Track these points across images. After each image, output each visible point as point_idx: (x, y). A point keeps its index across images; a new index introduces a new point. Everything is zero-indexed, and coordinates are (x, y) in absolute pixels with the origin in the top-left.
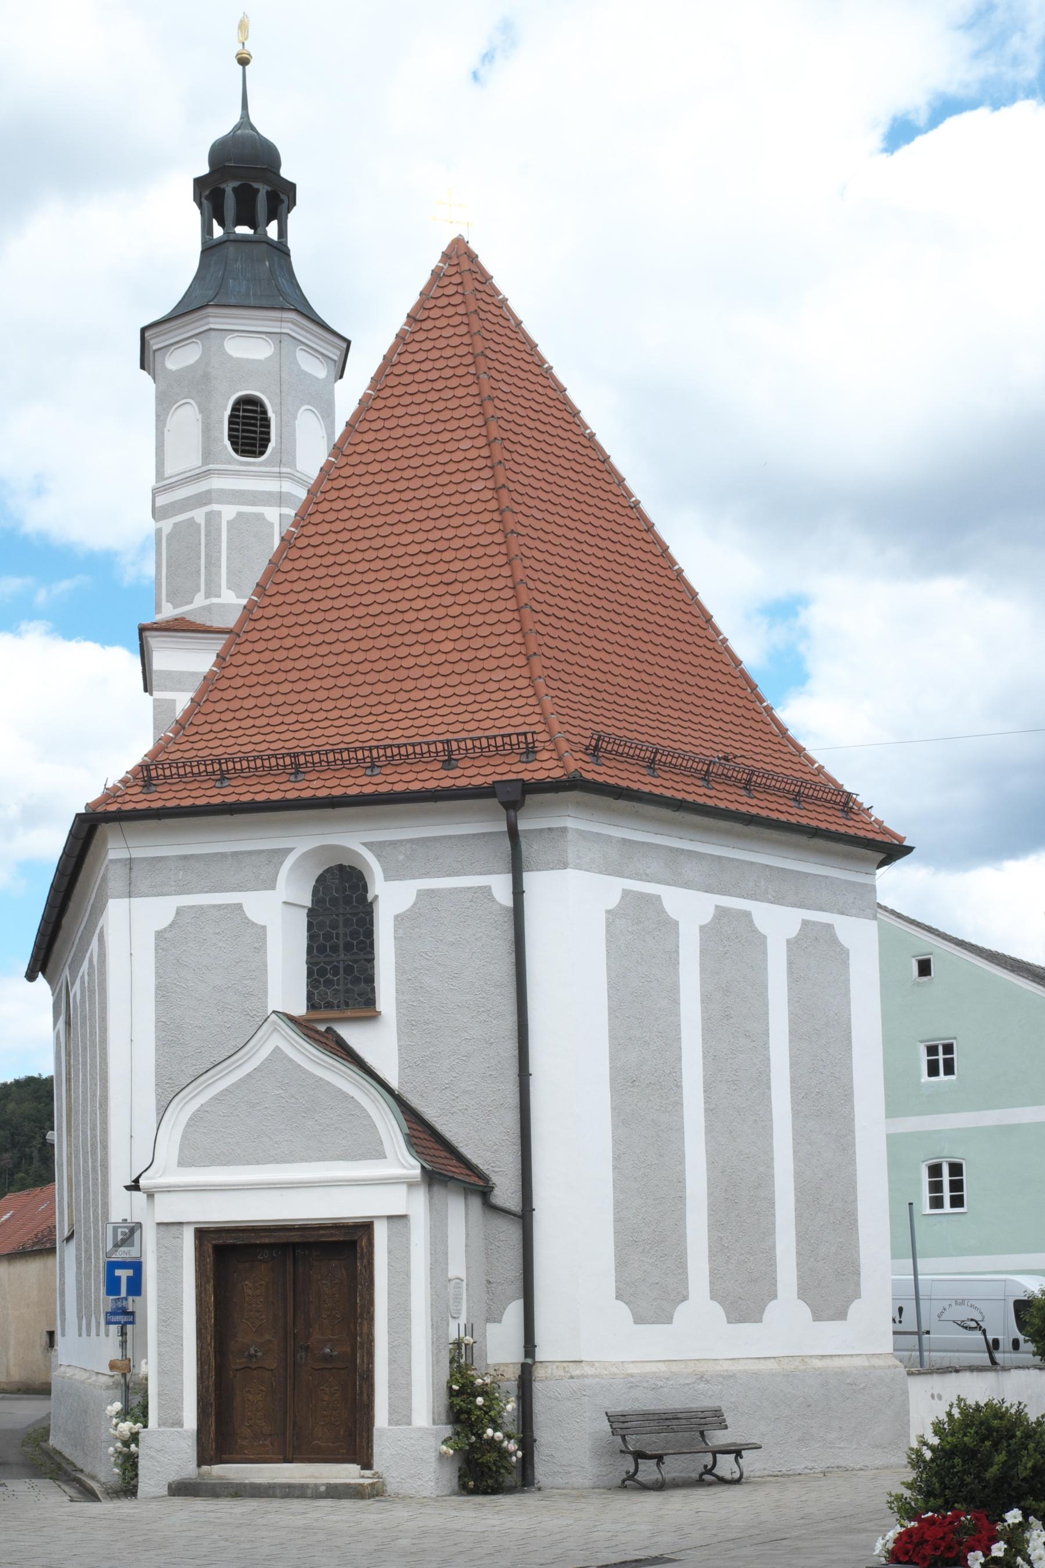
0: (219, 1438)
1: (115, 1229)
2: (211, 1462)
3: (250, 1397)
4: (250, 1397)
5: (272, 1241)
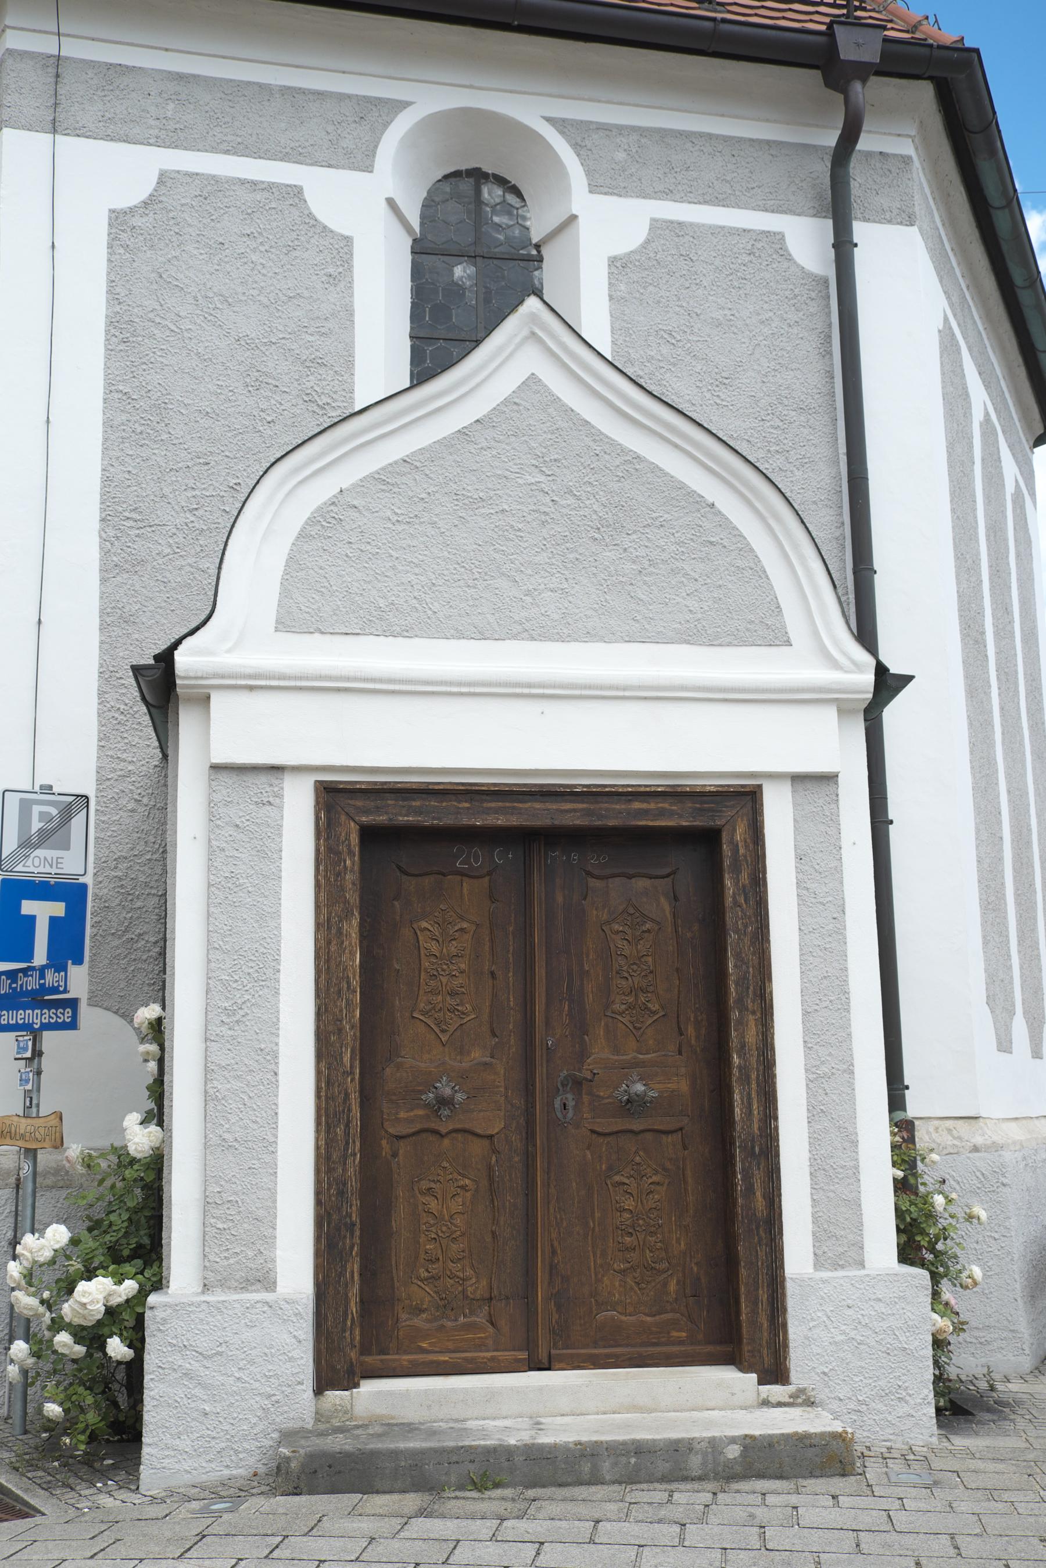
1: (25, 807)
3: (433, 1205)
4: (433, 1205)
5: (514, 821)
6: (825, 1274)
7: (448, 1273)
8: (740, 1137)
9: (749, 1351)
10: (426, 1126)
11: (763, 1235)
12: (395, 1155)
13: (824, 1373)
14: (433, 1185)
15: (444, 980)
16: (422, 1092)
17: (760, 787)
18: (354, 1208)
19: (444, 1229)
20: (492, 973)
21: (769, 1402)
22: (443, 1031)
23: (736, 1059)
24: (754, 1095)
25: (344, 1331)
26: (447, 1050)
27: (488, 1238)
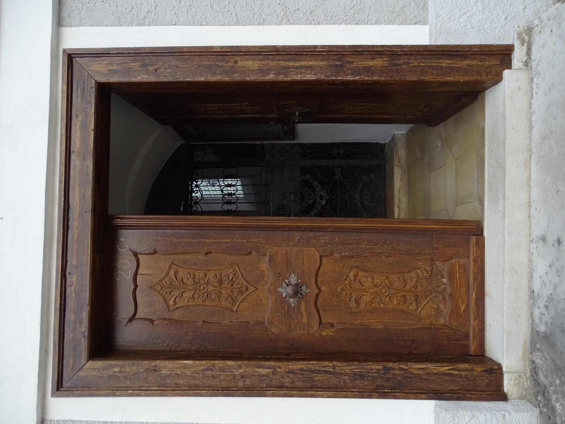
2: (495, 371)
3: (366, 298)
4: (366, 298)
6: (431, 15)
7: (413, 289)
8: (328, 76)
9: (487, 76)
10: (313, 303)
11: (402, 61)
12: (332, 325)
13: (506, 19)
14: (353, 298)
15: (211, 288)
16: (289, 306)
17: (64, 51)
18: (373, 367)
19: (383, 291)
20: (206, 254)
21: (526, 61)
22: (247, 289)
23: (271, 77)
24: (298, 64)
25: (461, 376)
26: (260, 287)
27: (391, 260)
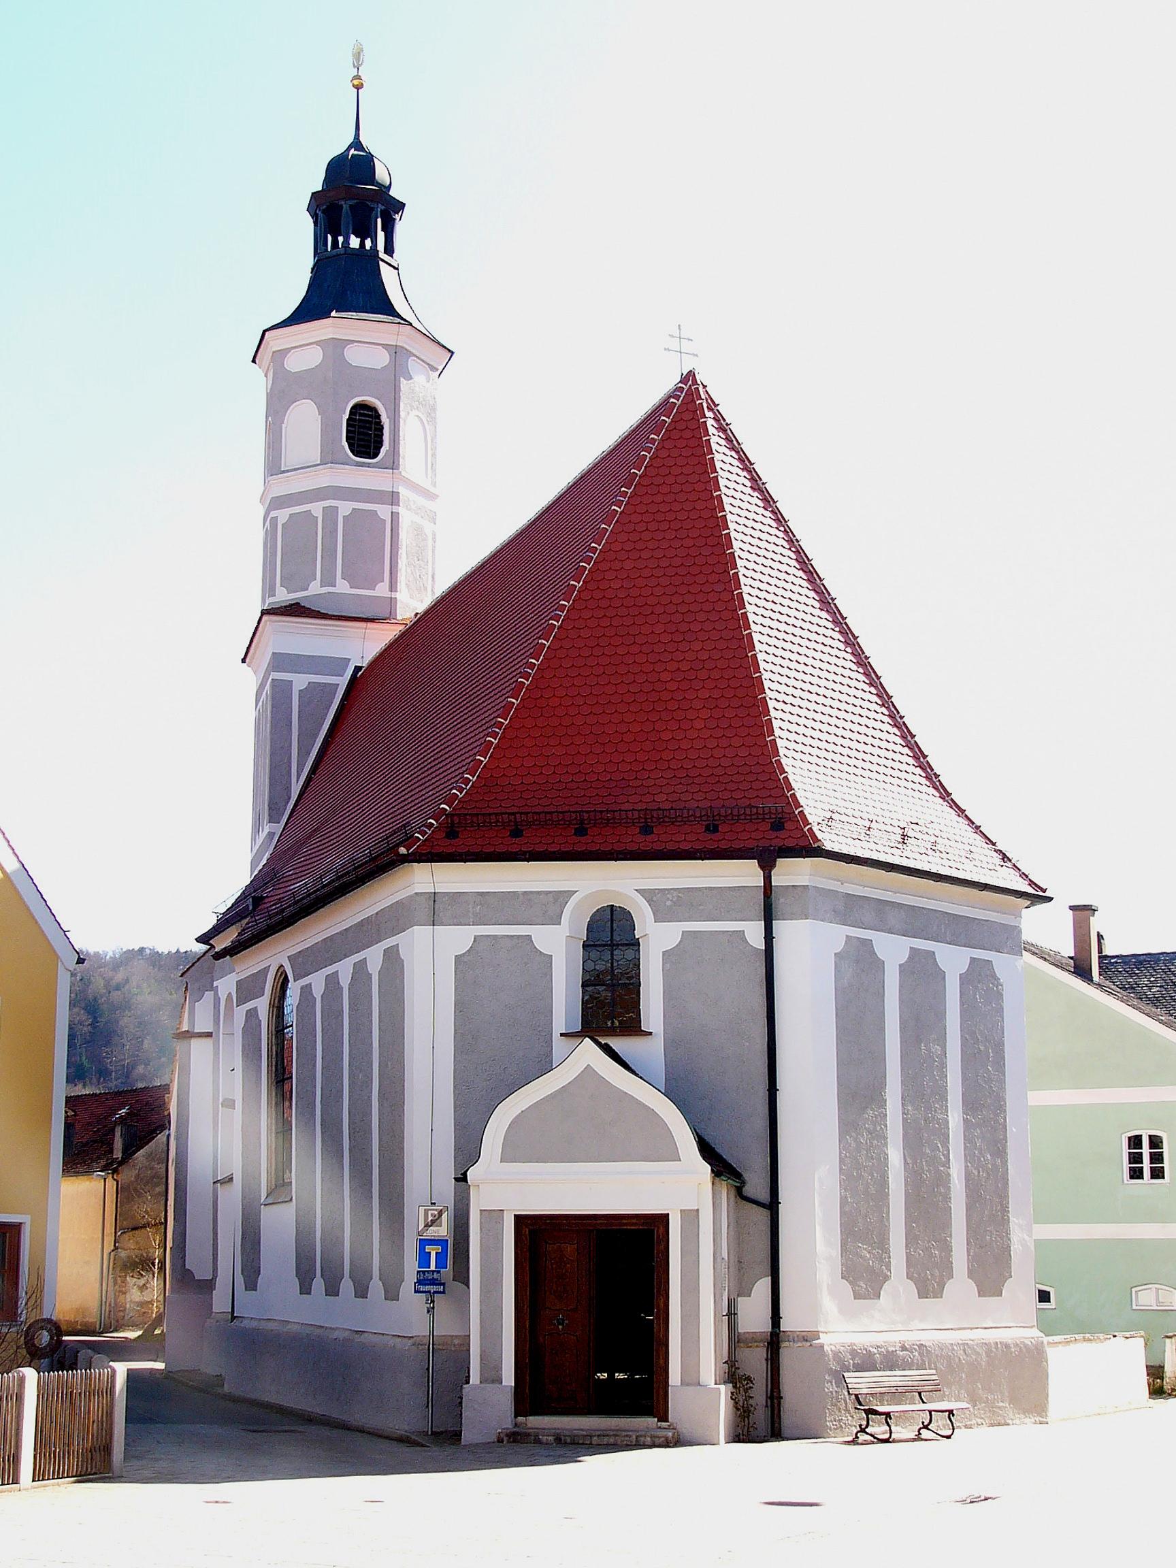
0: (530, 1397)
